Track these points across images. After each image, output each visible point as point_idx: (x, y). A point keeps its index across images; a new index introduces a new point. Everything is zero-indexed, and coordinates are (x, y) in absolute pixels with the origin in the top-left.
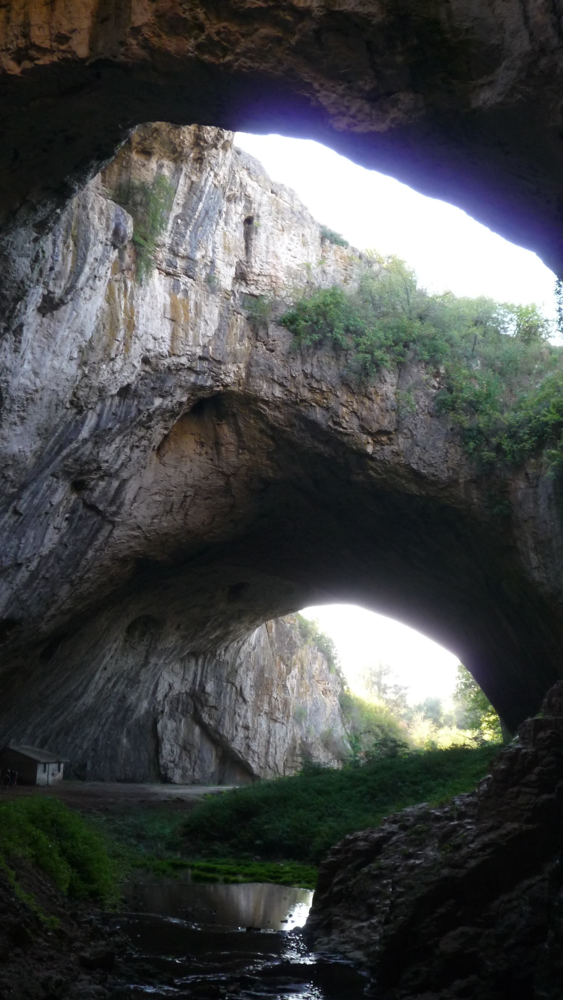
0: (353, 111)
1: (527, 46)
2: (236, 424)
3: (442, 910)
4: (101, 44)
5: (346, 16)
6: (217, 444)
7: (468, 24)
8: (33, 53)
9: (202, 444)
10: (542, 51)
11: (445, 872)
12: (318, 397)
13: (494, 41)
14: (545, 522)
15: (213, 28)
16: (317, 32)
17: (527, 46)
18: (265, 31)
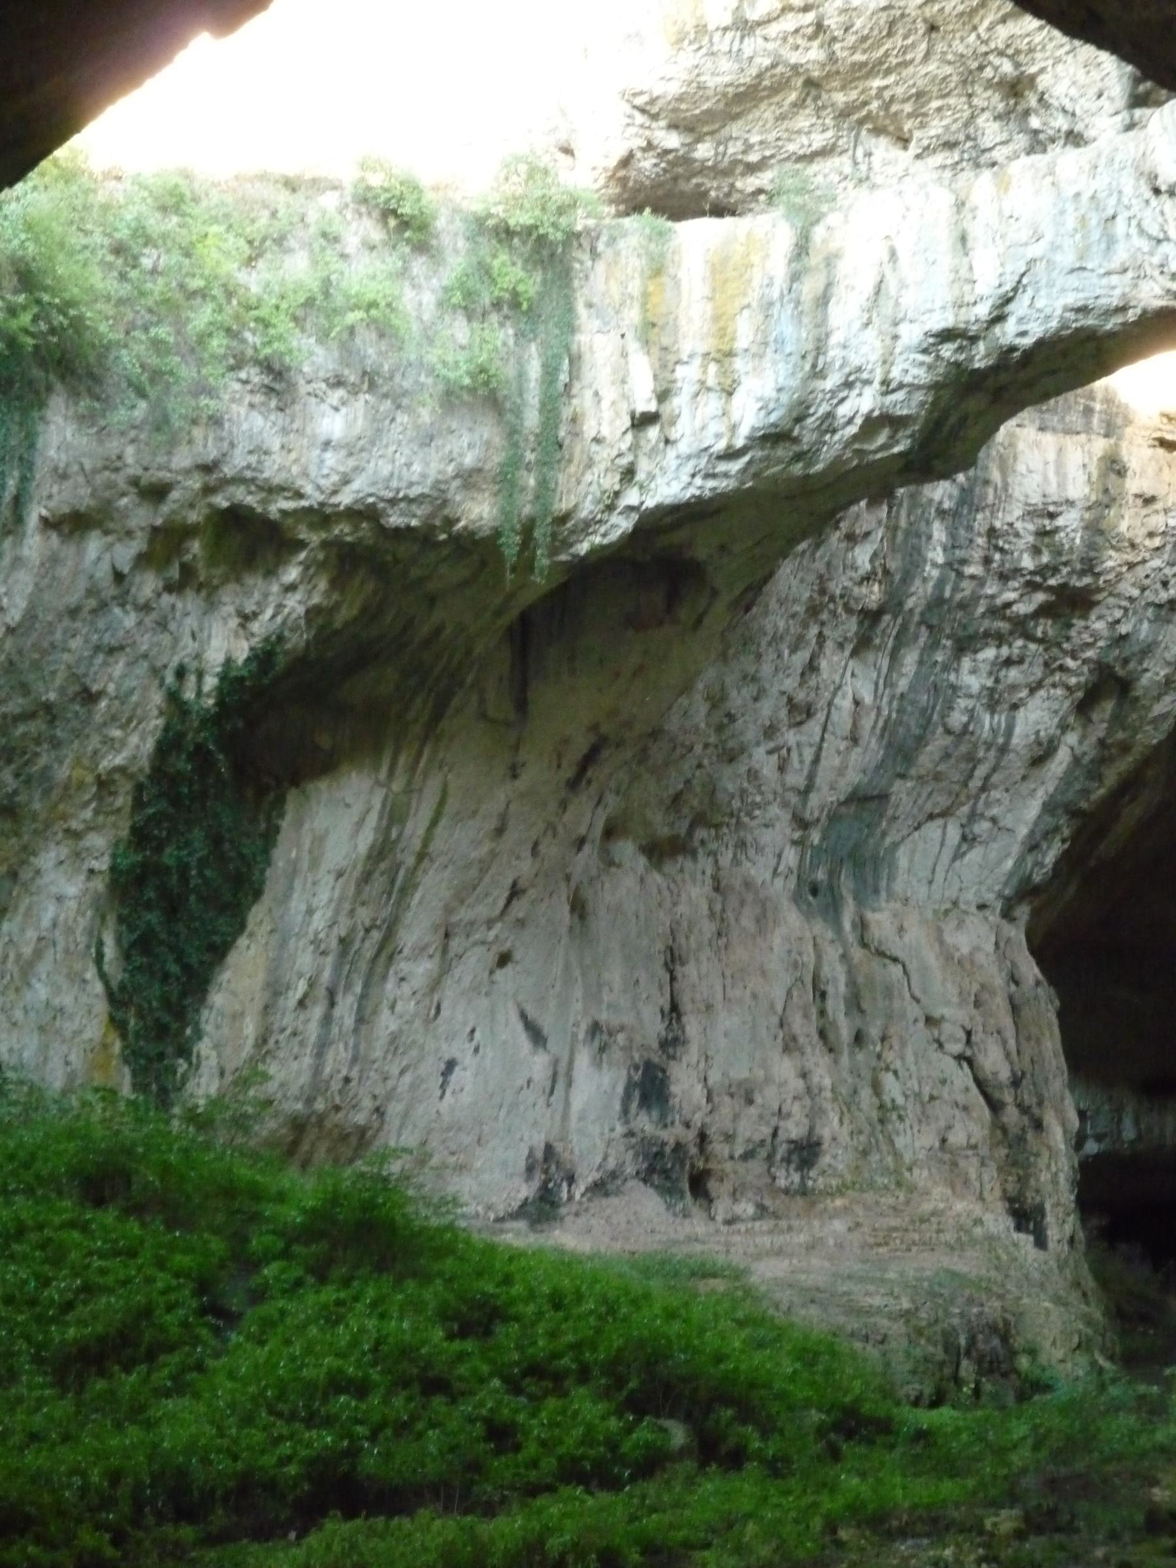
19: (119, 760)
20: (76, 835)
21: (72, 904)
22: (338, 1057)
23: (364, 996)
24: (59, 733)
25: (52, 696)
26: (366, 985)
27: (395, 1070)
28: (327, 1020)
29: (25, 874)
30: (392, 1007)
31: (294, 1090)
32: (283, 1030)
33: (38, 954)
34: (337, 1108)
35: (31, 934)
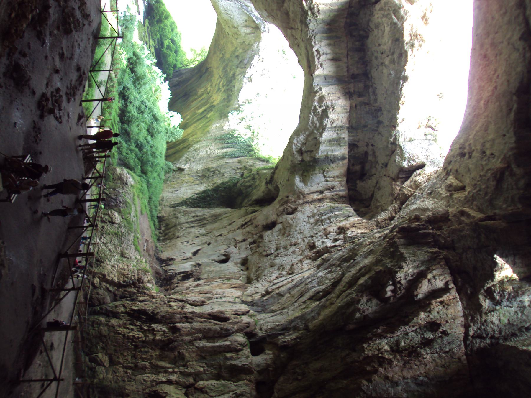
0: (298, 144)
1: (306, 193)
2: (253, 33)
3: (101, 276)
4: (318, 79)
5: (319, 148)
6: (246, 26)
7: (313, 177)
8: (318, 56)
9: (246, 21)
10: (304, 197)
11: (107, 274)
12: (262, 60)
13: (309, 184)
15: (319, 110)
16: (316, 138)
17: (306, 193)
18: (318, 124)
28: (192, 222)
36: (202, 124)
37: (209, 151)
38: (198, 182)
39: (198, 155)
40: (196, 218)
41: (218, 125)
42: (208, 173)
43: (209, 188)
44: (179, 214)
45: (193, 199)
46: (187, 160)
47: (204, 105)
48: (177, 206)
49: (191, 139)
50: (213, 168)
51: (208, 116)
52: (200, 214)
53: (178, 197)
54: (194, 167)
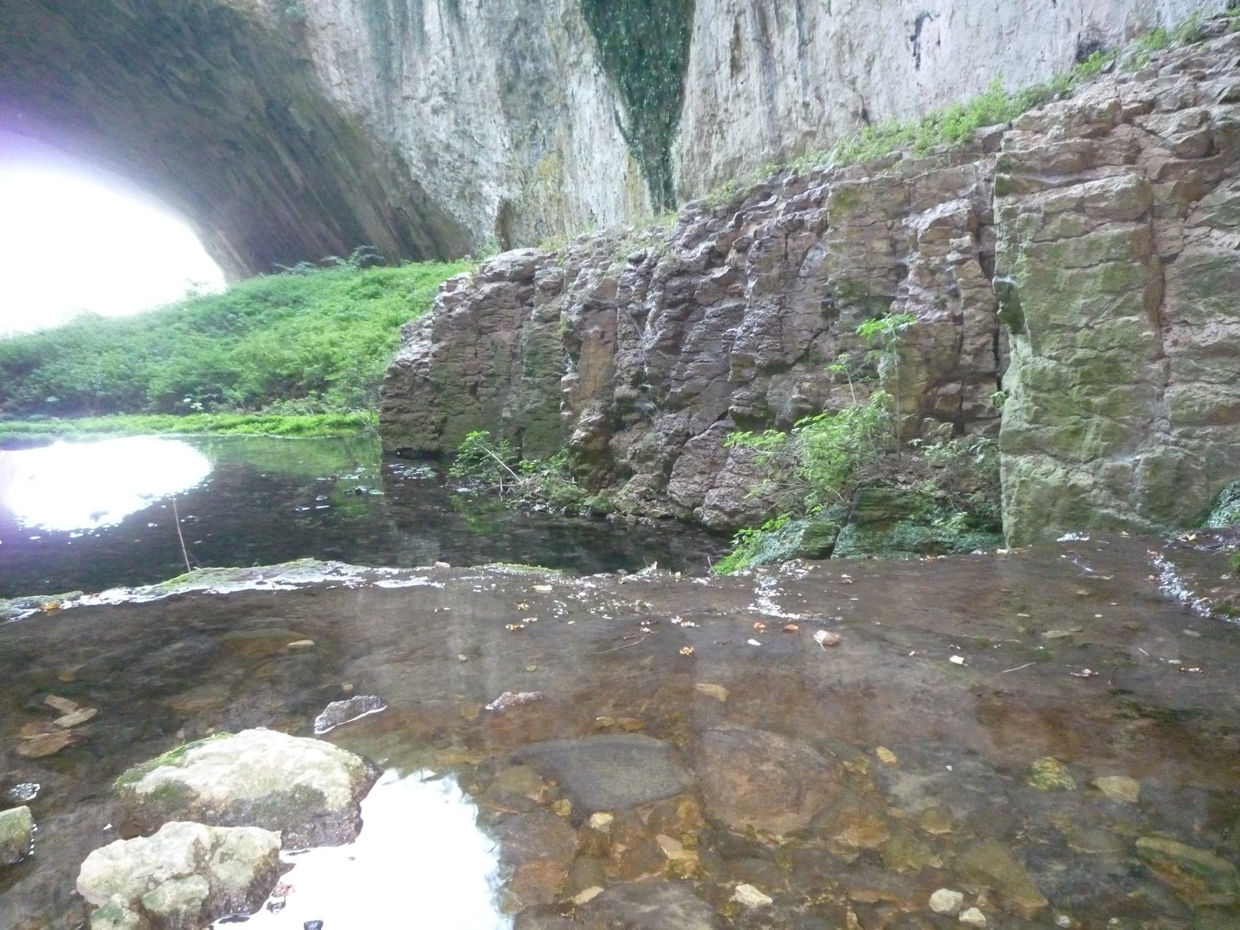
14: (348, 29)
19: (562, 11)
20: (577, 64)
21: (594, 101)
22: (789, 92)
23: (800, 20)
24: (534, 25)
25: (516, 13)
26: (800, 8)
27: (858, 67)
28: (767, 63)
29: (569, 101)
30: (829, 11)
31: (754, 140)
32: (726, 100)
33: (591, 138)
34: (812, 134)
35: (586, 130)
36: (340, 158)
37: (432, 102)
38: (560, 131)
39: (448, 148)
40: (750, 46)
41: (335, 75)
42: (521, 85)
43: (588, 58)
44: (716, 158)
45: (636, 119)
46: (469, 194)
47: (275, 161)
48: (668, 186)
49: (393, 197)
50: (500, 68)
51: (307, 129)
52: (725, 35)
53: (621, 204)
54: (498, 157)
